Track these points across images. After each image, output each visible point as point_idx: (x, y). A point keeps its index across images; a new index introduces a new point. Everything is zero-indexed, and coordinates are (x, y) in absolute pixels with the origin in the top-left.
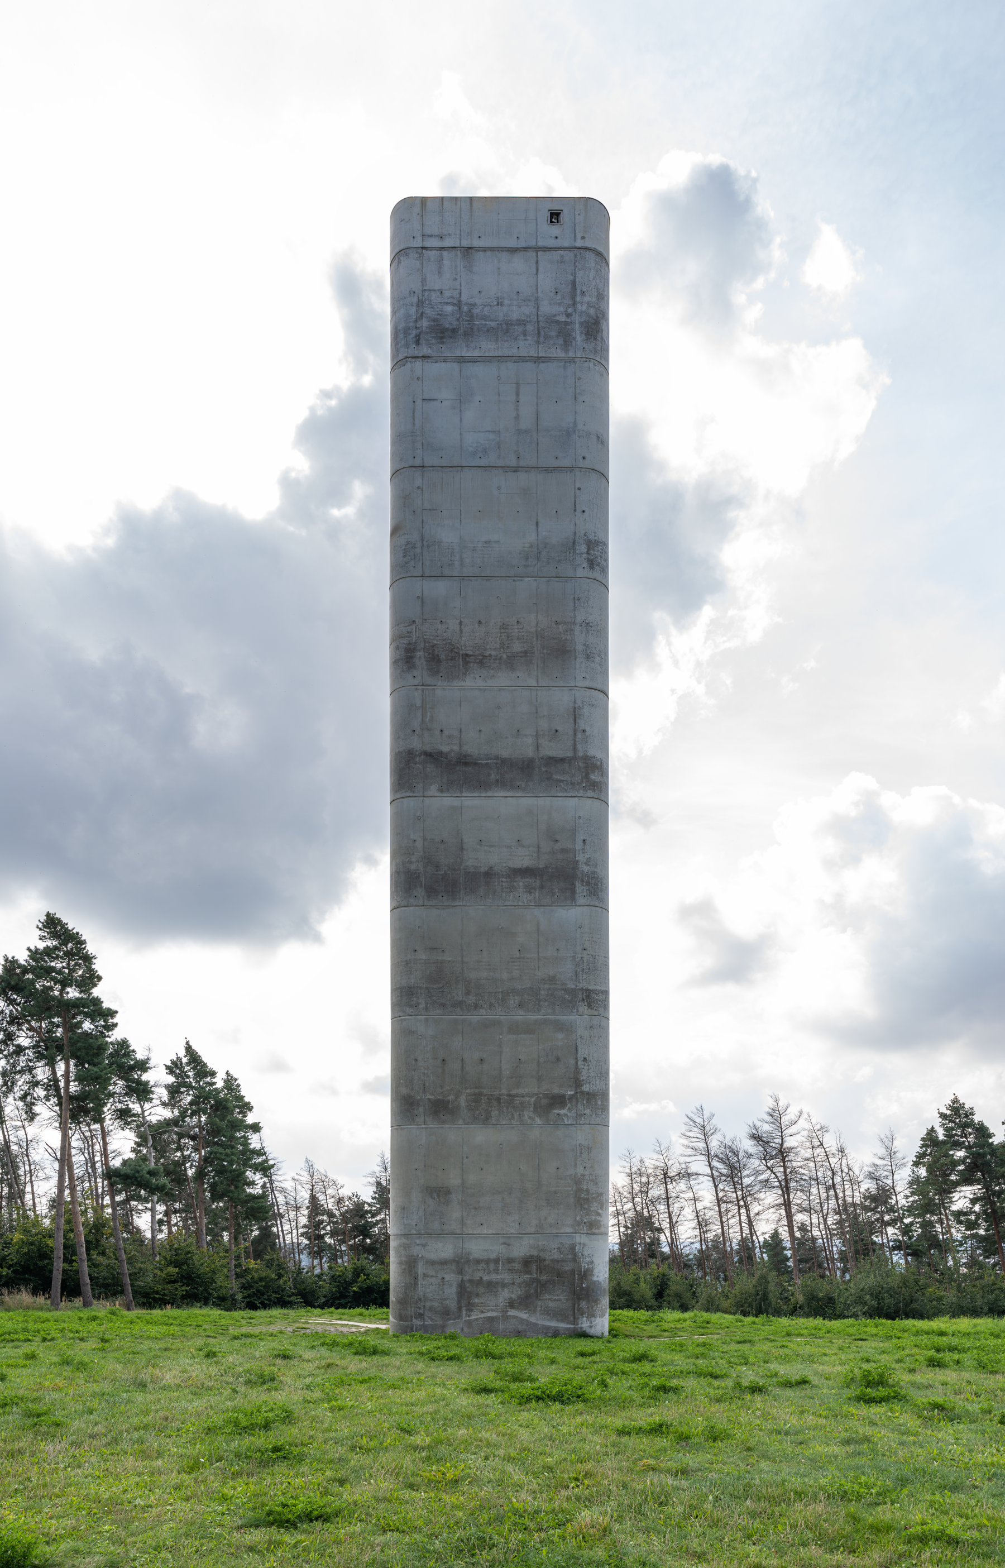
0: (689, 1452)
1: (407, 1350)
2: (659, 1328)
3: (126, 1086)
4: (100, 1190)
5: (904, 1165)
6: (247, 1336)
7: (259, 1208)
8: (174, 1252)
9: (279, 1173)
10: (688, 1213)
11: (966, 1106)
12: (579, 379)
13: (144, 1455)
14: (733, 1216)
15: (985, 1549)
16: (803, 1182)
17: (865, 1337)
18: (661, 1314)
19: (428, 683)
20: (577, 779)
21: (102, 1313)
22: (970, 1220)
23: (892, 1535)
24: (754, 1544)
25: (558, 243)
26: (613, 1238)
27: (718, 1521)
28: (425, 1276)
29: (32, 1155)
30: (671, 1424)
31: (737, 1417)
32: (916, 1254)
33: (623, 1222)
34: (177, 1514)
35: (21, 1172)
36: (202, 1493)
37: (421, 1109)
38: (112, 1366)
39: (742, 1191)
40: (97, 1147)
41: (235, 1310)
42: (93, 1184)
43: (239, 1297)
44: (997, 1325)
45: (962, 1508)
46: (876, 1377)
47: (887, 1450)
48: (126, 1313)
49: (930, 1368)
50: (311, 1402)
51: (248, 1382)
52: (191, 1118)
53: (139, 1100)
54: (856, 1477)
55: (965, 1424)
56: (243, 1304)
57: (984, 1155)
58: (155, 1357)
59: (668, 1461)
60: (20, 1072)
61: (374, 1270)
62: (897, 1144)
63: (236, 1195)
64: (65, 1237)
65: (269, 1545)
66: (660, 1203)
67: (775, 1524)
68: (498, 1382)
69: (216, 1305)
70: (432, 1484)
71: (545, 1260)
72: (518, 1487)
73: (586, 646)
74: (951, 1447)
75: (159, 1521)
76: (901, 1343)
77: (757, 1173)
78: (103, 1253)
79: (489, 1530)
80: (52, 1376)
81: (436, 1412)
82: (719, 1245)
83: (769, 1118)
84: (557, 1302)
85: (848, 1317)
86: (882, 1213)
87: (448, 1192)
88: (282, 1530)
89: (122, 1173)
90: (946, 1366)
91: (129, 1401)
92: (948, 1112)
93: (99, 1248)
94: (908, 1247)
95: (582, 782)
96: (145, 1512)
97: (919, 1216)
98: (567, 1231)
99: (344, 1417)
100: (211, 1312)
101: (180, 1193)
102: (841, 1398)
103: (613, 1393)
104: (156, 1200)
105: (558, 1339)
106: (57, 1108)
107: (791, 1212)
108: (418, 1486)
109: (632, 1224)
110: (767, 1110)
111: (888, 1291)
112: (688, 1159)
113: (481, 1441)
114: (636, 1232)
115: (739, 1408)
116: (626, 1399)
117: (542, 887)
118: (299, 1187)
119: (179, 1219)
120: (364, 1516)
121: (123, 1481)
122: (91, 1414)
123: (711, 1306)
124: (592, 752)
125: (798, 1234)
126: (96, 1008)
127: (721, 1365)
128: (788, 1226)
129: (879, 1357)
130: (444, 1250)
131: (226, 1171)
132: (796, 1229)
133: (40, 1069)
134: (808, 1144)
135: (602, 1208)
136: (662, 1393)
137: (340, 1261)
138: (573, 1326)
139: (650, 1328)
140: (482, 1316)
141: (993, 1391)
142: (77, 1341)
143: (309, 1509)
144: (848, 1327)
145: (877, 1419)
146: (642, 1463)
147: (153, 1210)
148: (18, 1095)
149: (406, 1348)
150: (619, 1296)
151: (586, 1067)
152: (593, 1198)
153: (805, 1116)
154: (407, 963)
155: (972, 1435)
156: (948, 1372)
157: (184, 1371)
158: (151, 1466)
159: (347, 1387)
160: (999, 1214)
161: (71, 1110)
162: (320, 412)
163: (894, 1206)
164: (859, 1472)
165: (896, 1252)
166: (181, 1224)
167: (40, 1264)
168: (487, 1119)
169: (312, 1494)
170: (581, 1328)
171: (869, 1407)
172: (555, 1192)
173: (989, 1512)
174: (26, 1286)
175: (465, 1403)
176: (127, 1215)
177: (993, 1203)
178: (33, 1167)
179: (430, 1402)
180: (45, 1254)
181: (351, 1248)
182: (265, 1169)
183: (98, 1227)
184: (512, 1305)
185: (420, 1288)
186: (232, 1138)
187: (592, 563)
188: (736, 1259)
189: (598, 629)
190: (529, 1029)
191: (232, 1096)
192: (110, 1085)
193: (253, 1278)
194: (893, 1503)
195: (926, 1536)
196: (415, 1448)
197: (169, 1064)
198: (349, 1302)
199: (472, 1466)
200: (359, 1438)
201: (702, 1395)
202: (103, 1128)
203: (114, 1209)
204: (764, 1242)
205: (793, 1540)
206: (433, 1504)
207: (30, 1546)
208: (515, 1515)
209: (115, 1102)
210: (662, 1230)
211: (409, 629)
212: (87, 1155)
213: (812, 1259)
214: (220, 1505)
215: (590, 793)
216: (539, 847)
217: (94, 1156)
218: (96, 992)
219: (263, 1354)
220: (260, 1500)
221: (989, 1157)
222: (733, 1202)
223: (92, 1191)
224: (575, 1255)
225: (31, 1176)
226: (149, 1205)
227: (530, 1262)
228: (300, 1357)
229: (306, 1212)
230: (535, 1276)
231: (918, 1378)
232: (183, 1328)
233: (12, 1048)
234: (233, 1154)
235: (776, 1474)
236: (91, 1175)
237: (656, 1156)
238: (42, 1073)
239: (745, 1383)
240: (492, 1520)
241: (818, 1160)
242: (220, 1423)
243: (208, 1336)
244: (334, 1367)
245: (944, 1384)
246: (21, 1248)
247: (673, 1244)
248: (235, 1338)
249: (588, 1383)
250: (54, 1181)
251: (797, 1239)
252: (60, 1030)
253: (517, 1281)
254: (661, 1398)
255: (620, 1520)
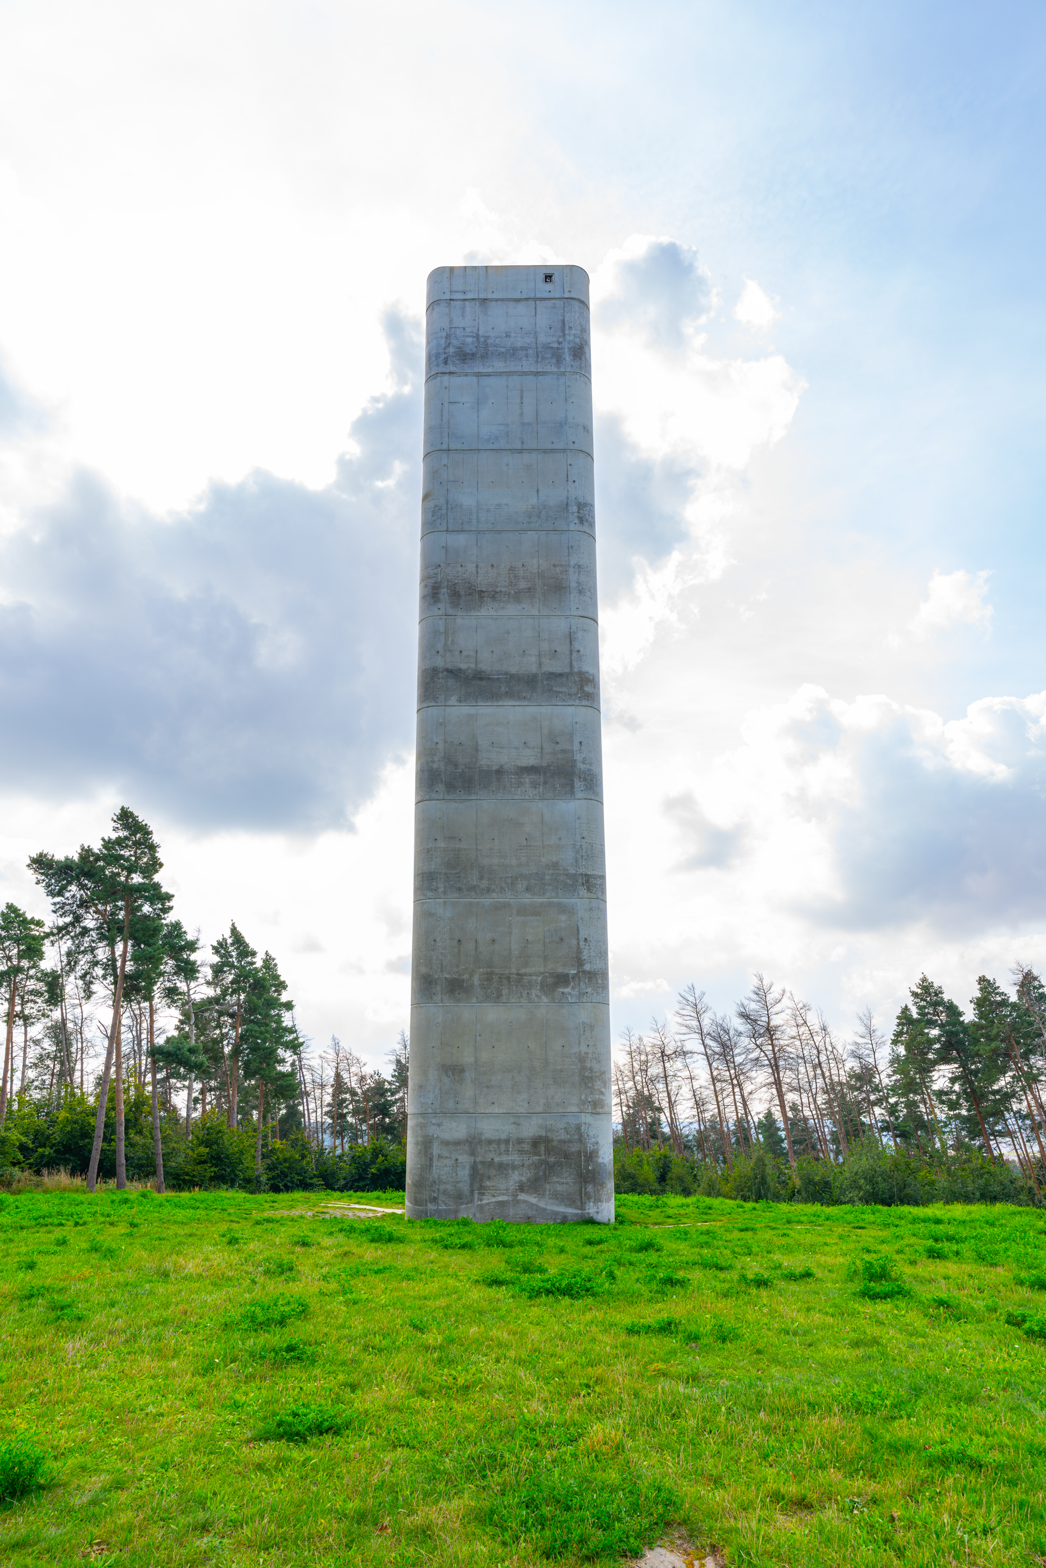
0: (699, 1355)
1: (421, 1236)
2: (663, 1214)
3: (176, 966)
4: (143, 1068)
5: (884, 1043)
6: (269, 1221)
7: (288, 1086)
8: (206, 1132)
9: (308, 1050)
10: (686, 1092)
11: (935, 985)
12: (569, 386)
13: (160, 1354)
14: (728, 1095)
15: (1010, 1474)
16: (791, 1061)
17: (863, 1225)
18: (664, 1199)
19: (450, 613)
20: (574, 690)
21: (133, 1196)
22: (951, 1099)
23: (912, 1456)
24: (771, 1466)
25: (552, 295)
26: (616, 1117)
27: (732, 1438)
28: (440, 1157)
29: (85, 1032)
30: (680, 1322)
31: (744, 1315)
32: (904, 1135)
33: (624, 1101)
34: (187, 1424)
35: (73, 1050)
36: (214, 1399)
37: (439, 988)
38: (139, 1254)
39: (735, 1069)
40: (145, 1025)
41: (260, 1192)
42: (137, 1061)
43: (264, 1179)
44: (990, 1213)
45: (981, 1424)
46: (879, 1270)
47: (897, 1354)
48: (156, 1195)
49: (931, 1260)
50: (326, 1295)
51: (267, 1272)
52: (231, 996)
53: (186, 979)
54: (869, 1386)
55: (973, 1324)
56: (267, 1187)
57: (956, 1034)
58: (180, 1243)
59: (678, 1365)
60: (83, 952)
61: (392, 1150)
62: (876, 1023)
63: (267, 1072)
64: (107, 1116)
65: (278, 1463)
66: (659, 1082)
67: (791, 1441)
68: (509, 1273)
69: (242, 1187)
70: (444, 1390)
71: (552, 1141)
72: (529, 1394)
73: (579, 583)
74: (961, 1351)
75: (169, 1433)
76: (899, 1231)
77: (748, 1051)
78: (140, 1132)
79: (500, 1447)
80: (80, 1264)
81: (448, 1307)
82: (716, 1125)
83: (755, 997)
84: (565, 1186)
85: (845, 1203)
86: (868, 1092)
87: (462, 1070)
88: (292, 1444)
89: (165, 1050)
90: (946, 1257)
91: (151, 1293)
92: (919, 991)
93: (137, 1127)
94: (895, 1128)
95: (578, 693)
96: (156, 1421)
97: (903, 1095)
98: (573, 1110)
99: (358, 1312)
100: (236, 1195)
101: (216, 1070)
102: (845, 1293)
103: (621, 1286)
104: (193, 1078)
105: (566, 1226)
106: (112, 987)
107: (782, 1091)
108: (430, 1393)
109: (633, 1103)
110: (753, 988)
111: (881, 1175)
112: (683, 1037)
113: (492, 1340)
114: (638, 1111)
115: (745, 1304)
116: (634, 1293)
117: (545, 783)
118: (325, 1065)
119: (213, 1097)
120: (374, 1429)
121: (137, 1385)
122: (113, 1307)
123: (712, 1191)
124: (585, 669)
125: (790, 1114)
126: (156, 892)
127: (725, 1256)
128: (781, 1106)
129: (879, 1247)
130: (457, 1129)
131: (259, 1049)
132: (788, 1109)
133: (101, 949)
134: (793, 1023)
135: (605, 1087)
136: (669, 1287)
137: (360, 1141)
138: (580, 1212)
139: (655, 1214)
140: (493, 1200)
141: (996, 1287)
142: (108, 1226)
143: (320, 1420)
144: (846, 1214)
145: (884, 1318)
146: (651, 1367)
147: (190, 1088)
148: (79, 974)
149: (420, 1235)
150: (624, 1179)
151: (587, 947)
152: (596, 1076)
153: (787, 994)
154: (429, 851)
155: (980, 1337)
156: (949, 1264)
157: (206, 1259)
158: (166, 1367)
159: (362, 1278)
160: (979, 1094)
161: (124, 989)
162: (370, 412)
163: (878, 1085)
164: (871, 1379)
165: (885, 1133)
166: (214, 1102)
167: (81, 1143)
168: (498, 998)
169: (323, 1402)
170: (588, 1213)
171: (875, 1304)
172: (561, 1071)
173: (1008, 1429)
174: (66, 1166)
175: (476, 1297)
176: (166, 1092)
177: (971, 1083)
178: (84, 1045)
179: (443, 1295)
180: (86, 1133)
181: (371, 1127)
182: (295, 1047)
183: (138, 1106)
184: (521, 1188)
185: (435, 1171)
186: (267, 1016)
187: (581, 520)
188: (733, 1141)
189: (588, 570)
190: (535, 911)
191: (269, 976)
192: (162, 964)
193: (278, 1159)
194: (909, 1418)
195: (947, 1458)
196: (427, 1348)
197: (215, 944)
198: (367, 1185)
199: (483, 1370)
200: (372, 1336)
201: (708, 1289)
202: (151, 1006)
203: (154, 1087)
204: (759, 1123)
205: (811, 1461)
206: (443, 1414)
207: (38, 1462)
208: (527, 1428)
209: (164, 981)
210: (662, 1109)
211: (435, 571)
212: (134, 1033)
213: (806, 1140)
214: (230, 1414)
215: (585, 703)
216: (542, 748)
217: (141, 1034)
218: (157, 878)
219: (283, 1240)
220: (271, 1408)
221: (962, 1035)
222: (725, 1081)
223: (136, 1068)
224: (581, 1135)
225: (82, 1054)
226: (187, 1083)
227: (539, 1142)
228: (319, 1244)
229: (330, 1090)
230: (544, 1157)
231: (919, 1270)
232: (209, 1212)
233: (78, 930)
234: (267, 1032)
235: (788, 1382)
236: (136, 1053)
237: (653, 1034)
238: (102, 953)
239: (750, 1276)
240: (503, 1434)
241: (803, 1038)
242: (238, 1318)
243: (232, 1221)
244: (351, 1255)
245: (946, 1278)
246: (65, 1126)
247: (672, 1124)
248: (258, 1223)
249: (596, 1274)
250: (102, 1059)
251: (790, 1119)
252: (122, 913)
253: (527, 1163)
254: (668, 1292)
255: (632, 1435)
